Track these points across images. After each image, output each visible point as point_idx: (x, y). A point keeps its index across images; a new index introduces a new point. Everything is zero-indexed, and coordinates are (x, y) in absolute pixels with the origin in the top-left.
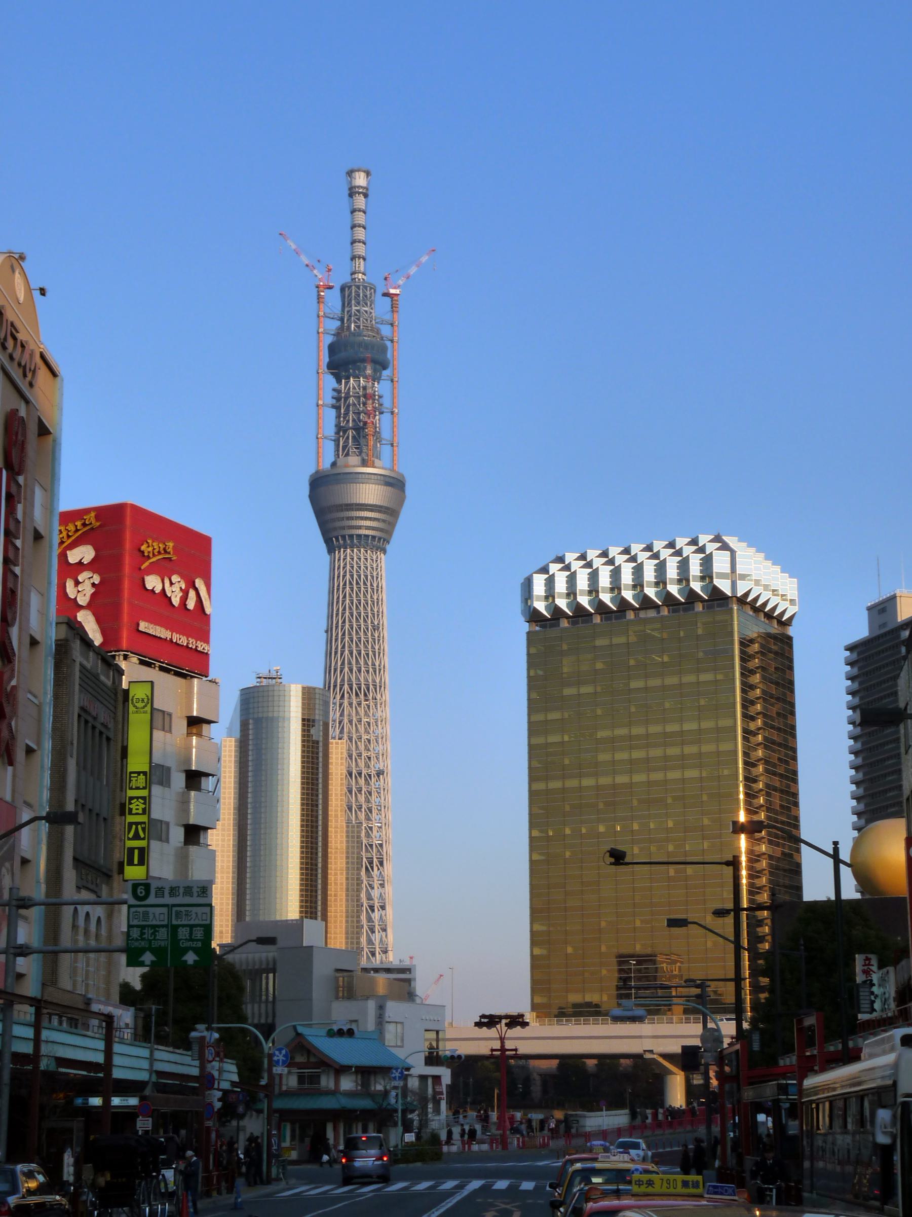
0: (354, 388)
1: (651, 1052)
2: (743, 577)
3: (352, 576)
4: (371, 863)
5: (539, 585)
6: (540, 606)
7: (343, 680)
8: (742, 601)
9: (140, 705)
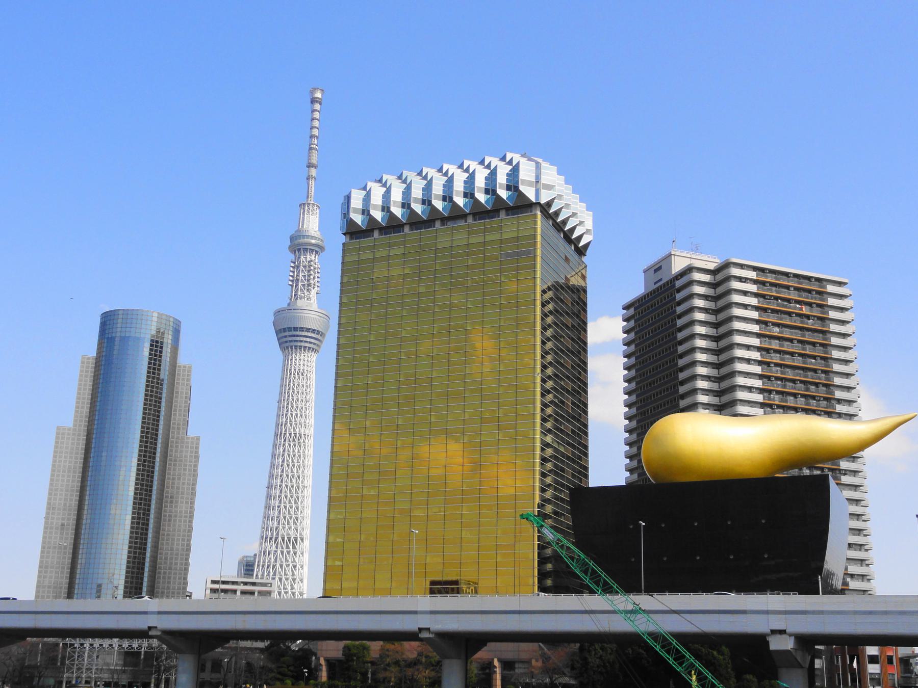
0: (303, 261)
1: (428, 629)
2: (549, 187)
3: (295, 370)
4: (296, 540)
5: (357, 201)
6: (358, 219)
7: (286, 431)
8: (545, 208)
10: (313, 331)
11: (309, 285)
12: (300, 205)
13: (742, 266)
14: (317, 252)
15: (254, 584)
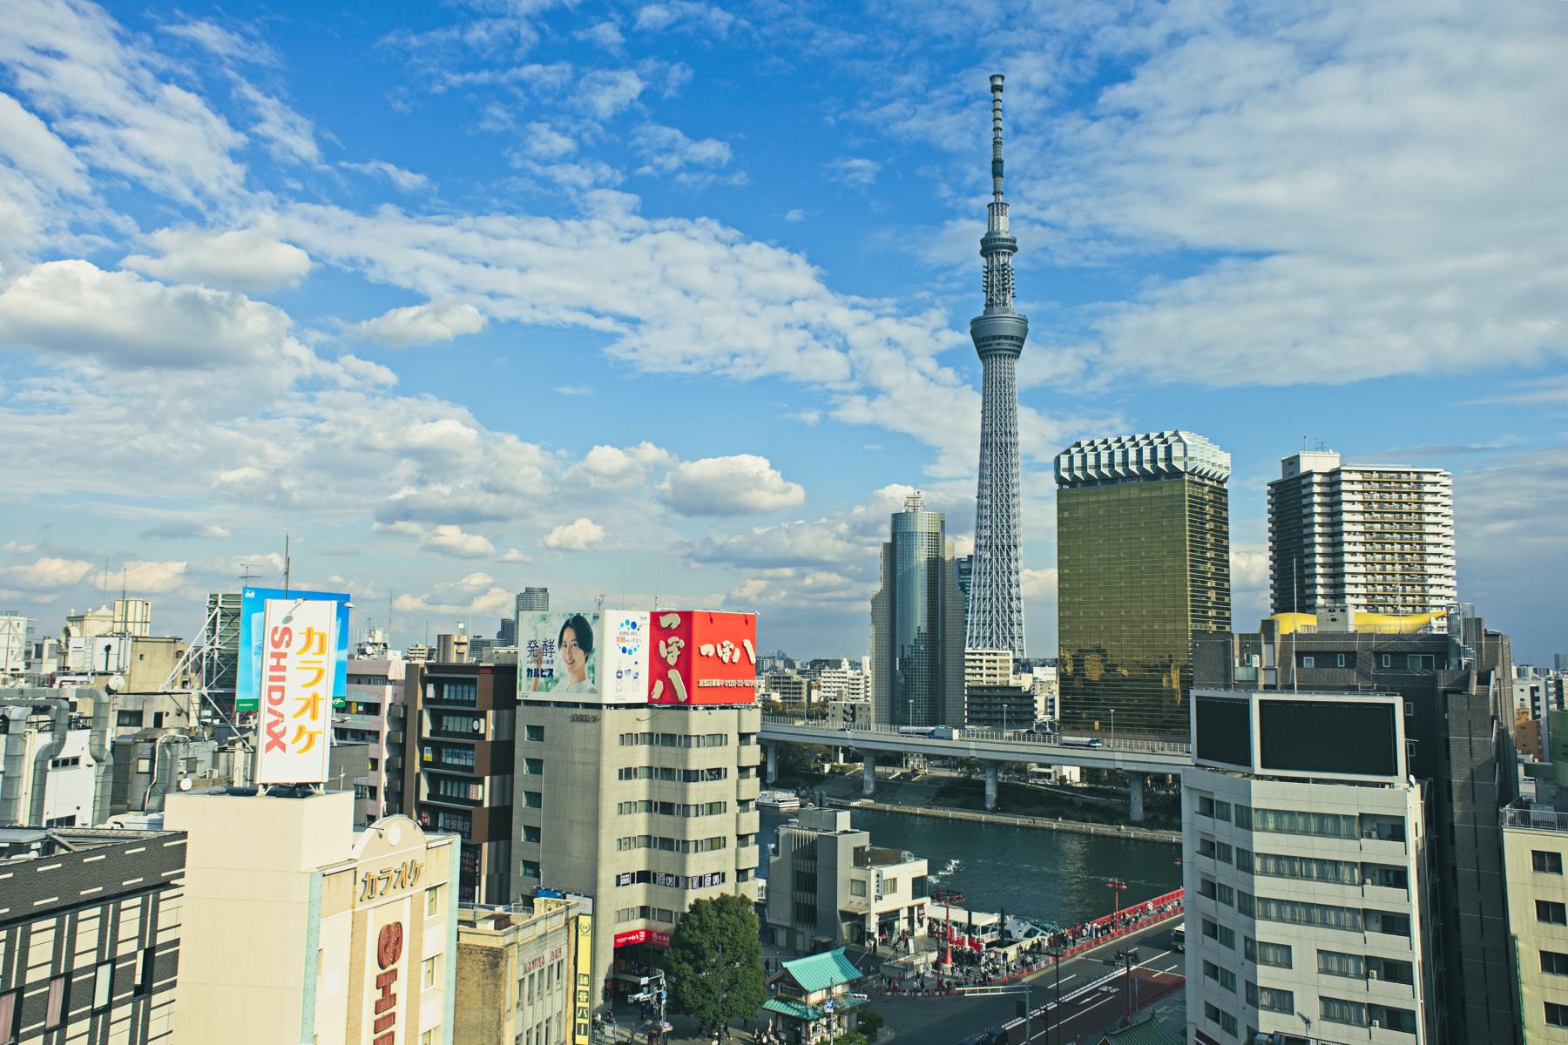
2: (1192, 459)
6: (1066, 475)
8: (1192, 473)
9: (585, 930)
10: (1012, 338)
11: (1004, 289)
12: (989, 206)
13: (1350, 472)
14: (1009, 254)
15: (995, 654)
